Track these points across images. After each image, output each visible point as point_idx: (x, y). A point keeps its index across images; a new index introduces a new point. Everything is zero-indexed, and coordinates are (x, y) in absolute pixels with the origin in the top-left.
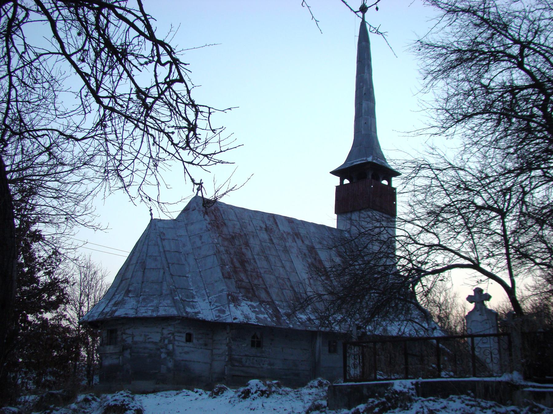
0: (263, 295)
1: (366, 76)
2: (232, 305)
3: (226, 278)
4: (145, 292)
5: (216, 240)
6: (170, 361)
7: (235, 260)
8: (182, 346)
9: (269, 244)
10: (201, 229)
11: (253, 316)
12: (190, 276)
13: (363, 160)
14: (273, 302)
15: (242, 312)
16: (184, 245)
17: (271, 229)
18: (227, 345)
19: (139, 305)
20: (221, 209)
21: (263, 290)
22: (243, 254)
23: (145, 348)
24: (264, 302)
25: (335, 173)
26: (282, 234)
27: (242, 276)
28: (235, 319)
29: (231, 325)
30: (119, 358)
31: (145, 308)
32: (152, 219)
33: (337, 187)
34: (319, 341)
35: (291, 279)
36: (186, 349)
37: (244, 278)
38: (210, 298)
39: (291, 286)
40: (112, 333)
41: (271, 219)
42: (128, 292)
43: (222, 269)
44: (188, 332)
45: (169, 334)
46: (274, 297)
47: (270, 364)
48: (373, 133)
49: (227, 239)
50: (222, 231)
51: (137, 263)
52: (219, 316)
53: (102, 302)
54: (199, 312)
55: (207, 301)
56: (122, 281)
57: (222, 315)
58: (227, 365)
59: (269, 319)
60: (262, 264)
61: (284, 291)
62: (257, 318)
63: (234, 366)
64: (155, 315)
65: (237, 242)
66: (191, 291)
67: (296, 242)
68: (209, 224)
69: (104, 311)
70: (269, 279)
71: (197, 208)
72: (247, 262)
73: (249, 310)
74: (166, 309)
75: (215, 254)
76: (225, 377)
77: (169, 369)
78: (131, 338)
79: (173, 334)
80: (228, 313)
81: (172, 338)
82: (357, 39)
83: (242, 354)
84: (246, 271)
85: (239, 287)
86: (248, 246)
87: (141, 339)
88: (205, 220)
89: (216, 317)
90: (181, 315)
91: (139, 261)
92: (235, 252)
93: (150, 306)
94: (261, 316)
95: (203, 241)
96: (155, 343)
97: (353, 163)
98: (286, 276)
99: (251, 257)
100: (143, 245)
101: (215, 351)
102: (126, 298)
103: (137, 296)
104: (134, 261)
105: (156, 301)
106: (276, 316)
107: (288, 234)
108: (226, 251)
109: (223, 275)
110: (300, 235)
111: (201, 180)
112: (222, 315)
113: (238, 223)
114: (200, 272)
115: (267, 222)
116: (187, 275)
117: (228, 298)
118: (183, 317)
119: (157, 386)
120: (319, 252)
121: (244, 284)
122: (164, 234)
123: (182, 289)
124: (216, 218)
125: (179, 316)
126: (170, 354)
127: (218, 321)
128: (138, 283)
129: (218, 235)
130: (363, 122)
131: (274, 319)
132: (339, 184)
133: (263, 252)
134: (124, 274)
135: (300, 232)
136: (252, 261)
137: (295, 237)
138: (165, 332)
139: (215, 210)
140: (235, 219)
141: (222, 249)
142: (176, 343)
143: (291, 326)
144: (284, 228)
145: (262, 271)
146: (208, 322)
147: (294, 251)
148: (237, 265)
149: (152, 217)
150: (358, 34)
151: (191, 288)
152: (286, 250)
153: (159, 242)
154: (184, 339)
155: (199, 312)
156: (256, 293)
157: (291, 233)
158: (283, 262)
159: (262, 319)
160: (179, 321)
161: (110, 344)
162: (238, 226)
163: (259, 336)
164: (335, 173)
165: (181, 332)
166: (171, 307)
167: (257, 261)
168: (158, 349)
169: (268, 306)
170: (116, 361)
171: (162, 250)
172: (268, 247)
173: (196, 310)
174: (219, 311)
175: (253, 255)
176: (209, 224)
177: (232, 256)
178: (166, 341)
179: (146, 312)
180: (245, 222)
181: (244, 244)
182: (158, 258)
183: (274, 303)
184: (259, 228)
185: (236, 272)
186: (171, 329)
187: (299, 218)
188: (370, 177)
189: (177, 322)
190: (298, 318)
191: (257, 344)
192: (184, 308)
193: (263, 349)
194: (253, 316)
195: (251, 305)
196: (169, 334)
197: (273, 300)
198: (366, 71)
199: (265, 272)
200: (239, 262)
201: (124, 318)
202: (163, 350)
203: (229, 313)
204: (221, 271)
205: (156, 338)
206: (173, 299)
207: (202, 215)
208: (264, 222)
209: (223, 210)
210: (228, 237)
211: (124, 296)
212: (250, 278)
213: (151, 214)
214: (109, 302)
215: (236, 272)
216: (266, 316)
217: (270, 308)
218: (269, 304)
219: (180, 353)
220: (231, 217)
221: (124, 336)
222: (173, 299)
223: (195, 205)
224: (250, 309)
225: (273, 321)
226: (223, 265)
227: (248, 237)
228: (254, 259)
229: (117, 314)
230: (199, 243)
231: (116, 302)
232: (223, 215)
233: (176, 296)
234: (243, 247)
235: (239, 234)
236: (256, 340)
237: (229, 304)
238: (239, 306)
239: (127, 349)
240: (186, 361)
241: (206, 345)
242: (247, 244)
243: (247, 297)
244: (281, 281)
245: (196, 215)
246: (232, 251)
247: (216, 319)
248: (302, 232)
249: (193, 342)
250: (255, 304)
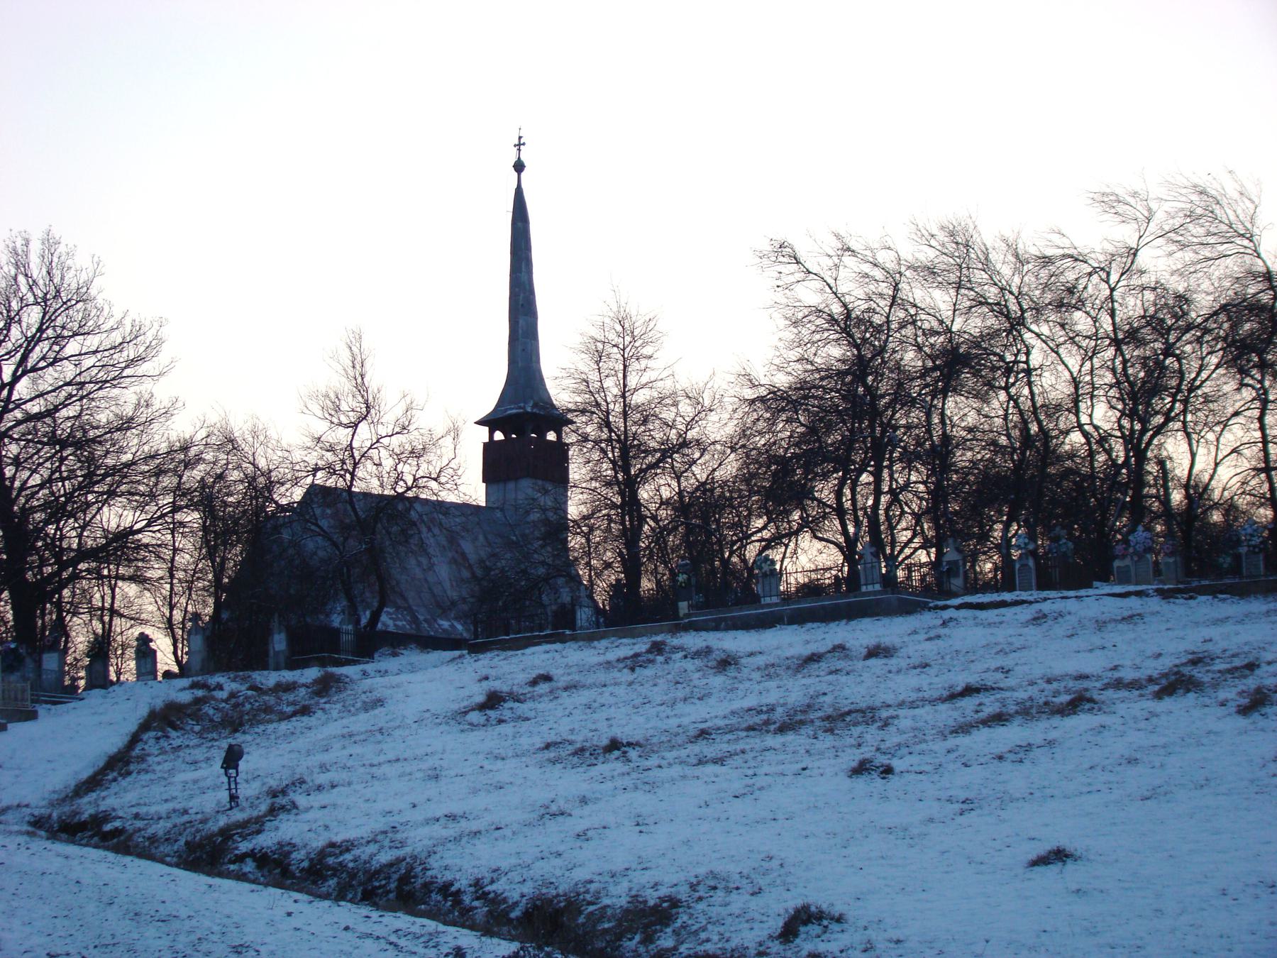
0: (399, 602)
1: (524, 277)
14: (410, 607)
25: (481, 423)
33: (485, 444)
82: (510, 215)
94: (400, 623)
130: (520, 348)
164: (481, 423)
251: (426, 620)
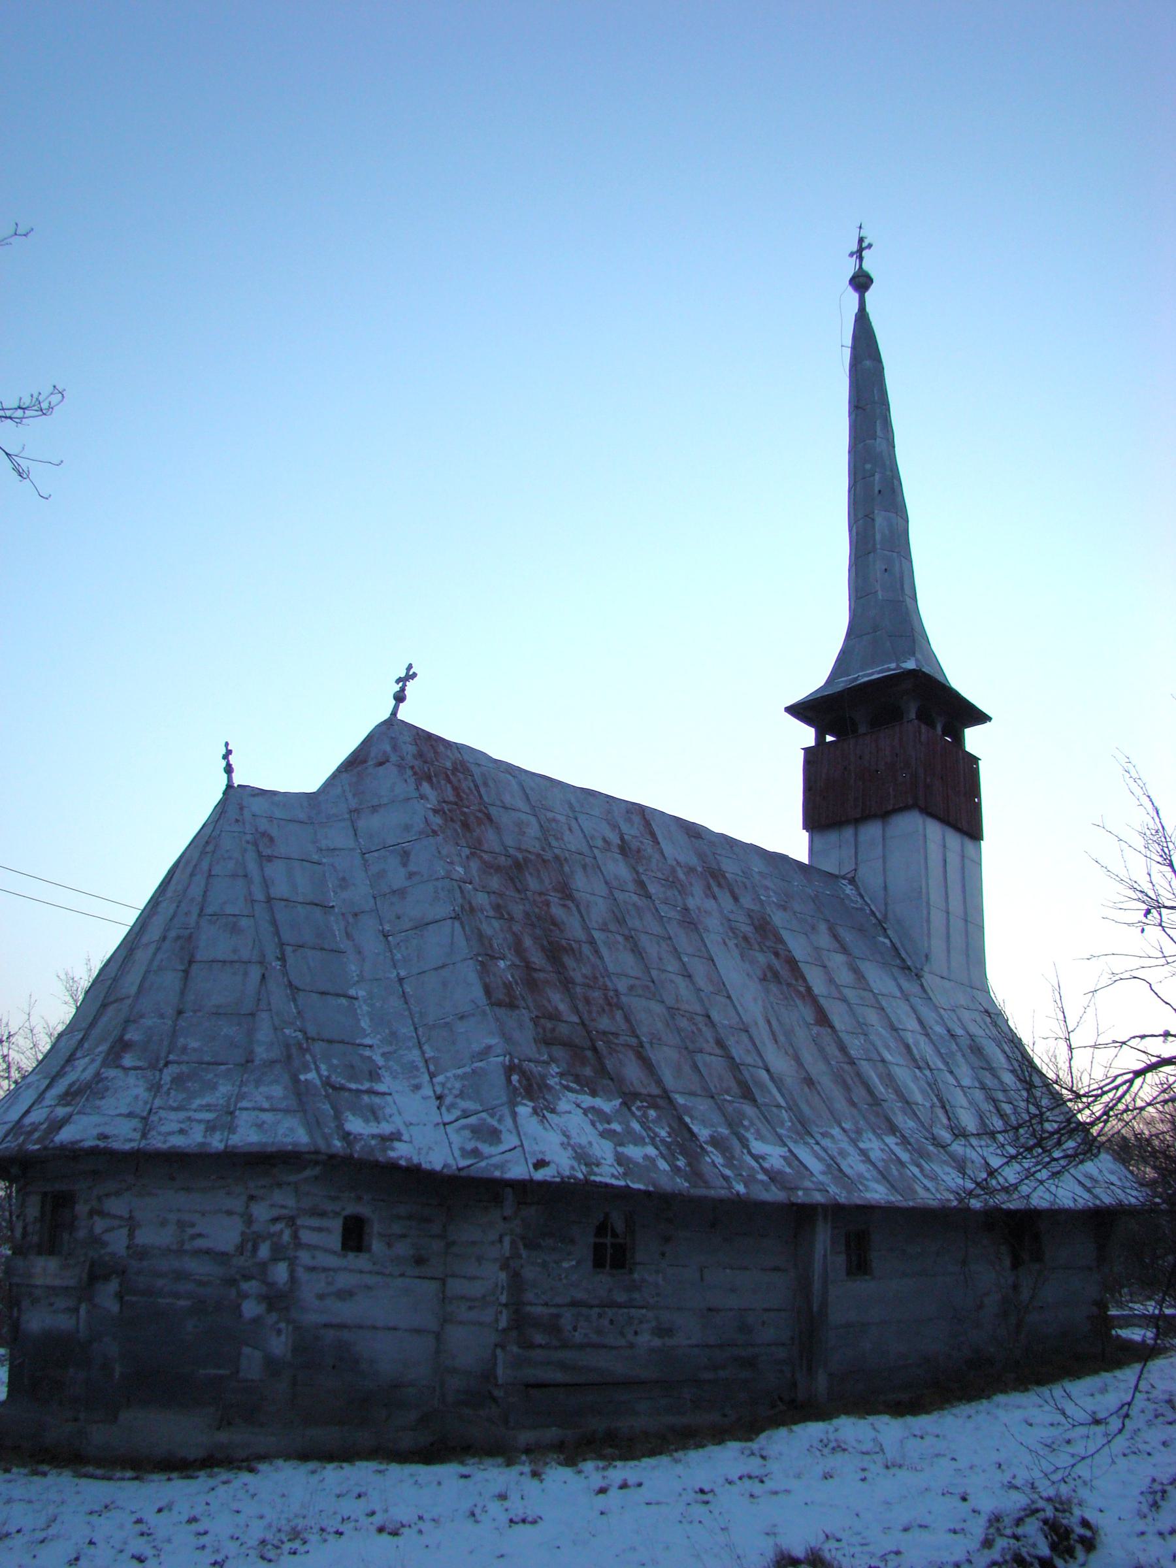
0: (633, 1072)
2: (524, 1110)
3: (499, 1004)
4: (184, 1049)
5: (460, 870)
6: (279, 1332)
7: (528, 942)
8: (325, 1270)
9: (635, 898)
10: (407, 828)
11: (604, 1150)
12: (361, 993)
13: (889, 669)
14: (666, 1095)
15: (564, 1138)
16: (344, 883)
17: (639, 851)
18: (505, 1266)
19: (158, 1102)
20: (474, 769)
21: (631, 1055)
22: (554, 923)
23: (180, 1276)
24: (636, 1095)
25: (800, 711)
26: (673, 871)
27: (557, 1000)
28: (540, 1164)
29: (523, 1188)
30: (77, 1310)
31: (182, 1115)
32: (230, 786)
33: (807, 751)
34: (823, 1238)
35: (714, 1015)
36: (344, 1281)
37: (562, 1007)
38: (440, 1079)
39: (720, 1043)
40: (59, 1206)
41: (637, 819)
42: (121, 1046)
43: (484, 969)
44: (351, 1209)
45: (275, 1220)
46: (669, 1080)
47: (663, 1331)
48: (908, 600)
49: (498, 869)
50: (480, 842)
51: (164, 938)
52: (475, 1152)
53: (29, 1086)
54: (396, 1136)
55: (427, 1091)
56: (105, 1005)
57: (486, 1149)
58: (503, 1347)
59: (663, 1165)
60: (619, 962)
61: (699, 1058)
62: (620, 1159)
63: (531, 1346)
64: (217, 1143)
65: (533, 883)
66: (367, 1053)
67: (715, 898)
68: (435, 811)
69: (27, 1121)
70: (648, 1015)
71: (394, 758)
72: (570, 950)
73: (589, 1128)
74: (264, 1121)
75: (457, 917)
76: (498, 1393)
77: (272, 1365)
78: (124, 1231)
79: (291, 1221)
80: (510, 1140)
81: (286, 1237)
82: (847, 353)
83: (558, 1300)
84: (567, 984)
85: (547, 1041)
86: (570, 897)
87: (163, 1237)
88: (422, 797)
89: (465, 1153)
90: (322, 1146)
91: (172, 934)
92: (527, 914)
93: (202, 1108)
94: (634, 1152)
95: (412, 867)
96: (221, 1257)
97: (856, 679)
98: (698, 1008)
99: (580, 934)
100: (192, 875)
101: (456, 1286)
102: (111, 1073)
103: (153, 1066)
104: (154, 933)
105: (225, 1089)
106: (684, 1152)
107: (691, 870)
108: (497, 908)
109: (488, 991)
110: (724, 877)
111: (410, 667)
112: (486, 1149)
113: (533, 820)
114: (401, 980)
115: (625, 828)
116: (352, 992)
117: (509, 1081)
118: (332, 1157)
119: (223, 1437)
120: (785, 934)
121: (563, 1030)
122: (272, 839)
123: (330, 1041)
124: (458, 795)
125: (317, 1152)
126: (278, 1300)
127: (473, 1172)
128: (162, 1016)
129: (467, 851)
130: (879, 566)
131: (681, 1163)
132: (811, 742)
133: (621, 921)
134: (115, 980)
135: (724, 867)
136: (586, 949)
137: (711, 881)
138: (261, 1212)
139: (455, 770)
140: (521, 804)
141: (481, 899)
142: (304, 1257)
143: (740, 1188)
144: (676, 851)
146: (432, 1175)
147: (713, 923)
148: (537, 959)
149: (230, 779)
150: (848, 341)
151: (368, 1041)
152: (690, 922)
153: (252, 866)
154: (334, 1240)
155: (396, 1136)
156: (609, 1064)
157: (699, 869)
158: (685, 959)
159: (637, 1164)
160: (317, 1170)
161: (50, 1247)
162: (533, 830)
163: (620, 1226)
164: (800, 711)
165: (323, 1214)
166: (287, 1111)
167: (604, 951)
168: (231, 1282)
169: (652, 1113)
170: (64, 1322)
171: (259, 895)
172: (634, 905)
173: (386, 1128)
174: (476, 1131)
175: (586, 928)
176: (435, 811)
177: (516, 928)
178: (264, 1251)
179: (182, 1129)
180: (554, 820)
181: (555, 890)
182: (244, 922)
183: (670, 1101)
184: (600, 843)
185: (532, 985)
186: (286, 1200)
187: (717, 825)
188: (913, 715)
189: (308, 1173)
190: (756, 1158)
191: (612, 1256)
192: (338, 1116)
193: (636, 1276)
194: (604, 1150)
196: (275, 1220)
197: (665, 1091)
198: (879, 433)
199: (631, 988)
200: (543, 949)
201: (94, 1152)
202: (249, 1286)
203: (516, 1142)
204: (481, 978)
205: (224, 1234)
206: (295, 1080)
207: (412, 780)
208: (615, 826)
209: (483, 775)
210: (502, 860)
211: (104, 1064)
212: (580, 1006)
213: (229, 769)
214: (48, 1087)
215: (532, 985)
216: (651, 1151)
217: (659, 1117)
218: (656, 1107)
219: (321, 1297)
220: (508, 799)
221: (99, 1225)
222: (295, 1080)
223: (388, 748)
224: (593, 1124)
225: (676, 1170)
226: (486, 958)
227: (566, 869)
228: (592, 942)
229: (66, 1135)
230: (397, 877)
231: (71, 1085)
232: (483, 790)
233: (307, 1069)
234: (554, 898)
235: (538, 855)
236: (608, 1240)
237: (512, 1104)
238: (553, 1111)
239: (106, 1278)
240: (342, 1326)
241: (419, 1261)
242: (566, 892)
243: (577, 1079)
244: (684, 1023)
245: (388, 782)
246: (518, 910)
247: (463, 1163)
248: (730, 868)
249: (369, 1250)
250: (608, 1106)
251: (715, 1141)
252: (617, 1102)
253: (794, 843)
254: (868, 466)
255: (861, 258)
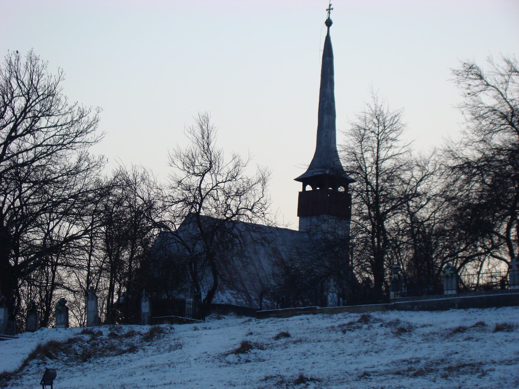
0: (240, 286)
1: (328, 91)
11: (233, 300)
25: (298, 179)
28: (222, 301)
33: (300, 193)
39: (260, 280)
46: (247, 287)
59: (244, 303)
62: (236, 301)
94: (239, 300)
131: (248, 303)
132: (301, 190)
145: (239, 268)
150: (323, 49)
164: (298, 179)
195: (232, 293)
198: (328, 86)
216: (242, 300)
243: (229, 288)
244: (251, 276)
250: (234, 292)
252: (236, 292)
253: (292, 222)
254: (324, 99)
255: (329, 13)
